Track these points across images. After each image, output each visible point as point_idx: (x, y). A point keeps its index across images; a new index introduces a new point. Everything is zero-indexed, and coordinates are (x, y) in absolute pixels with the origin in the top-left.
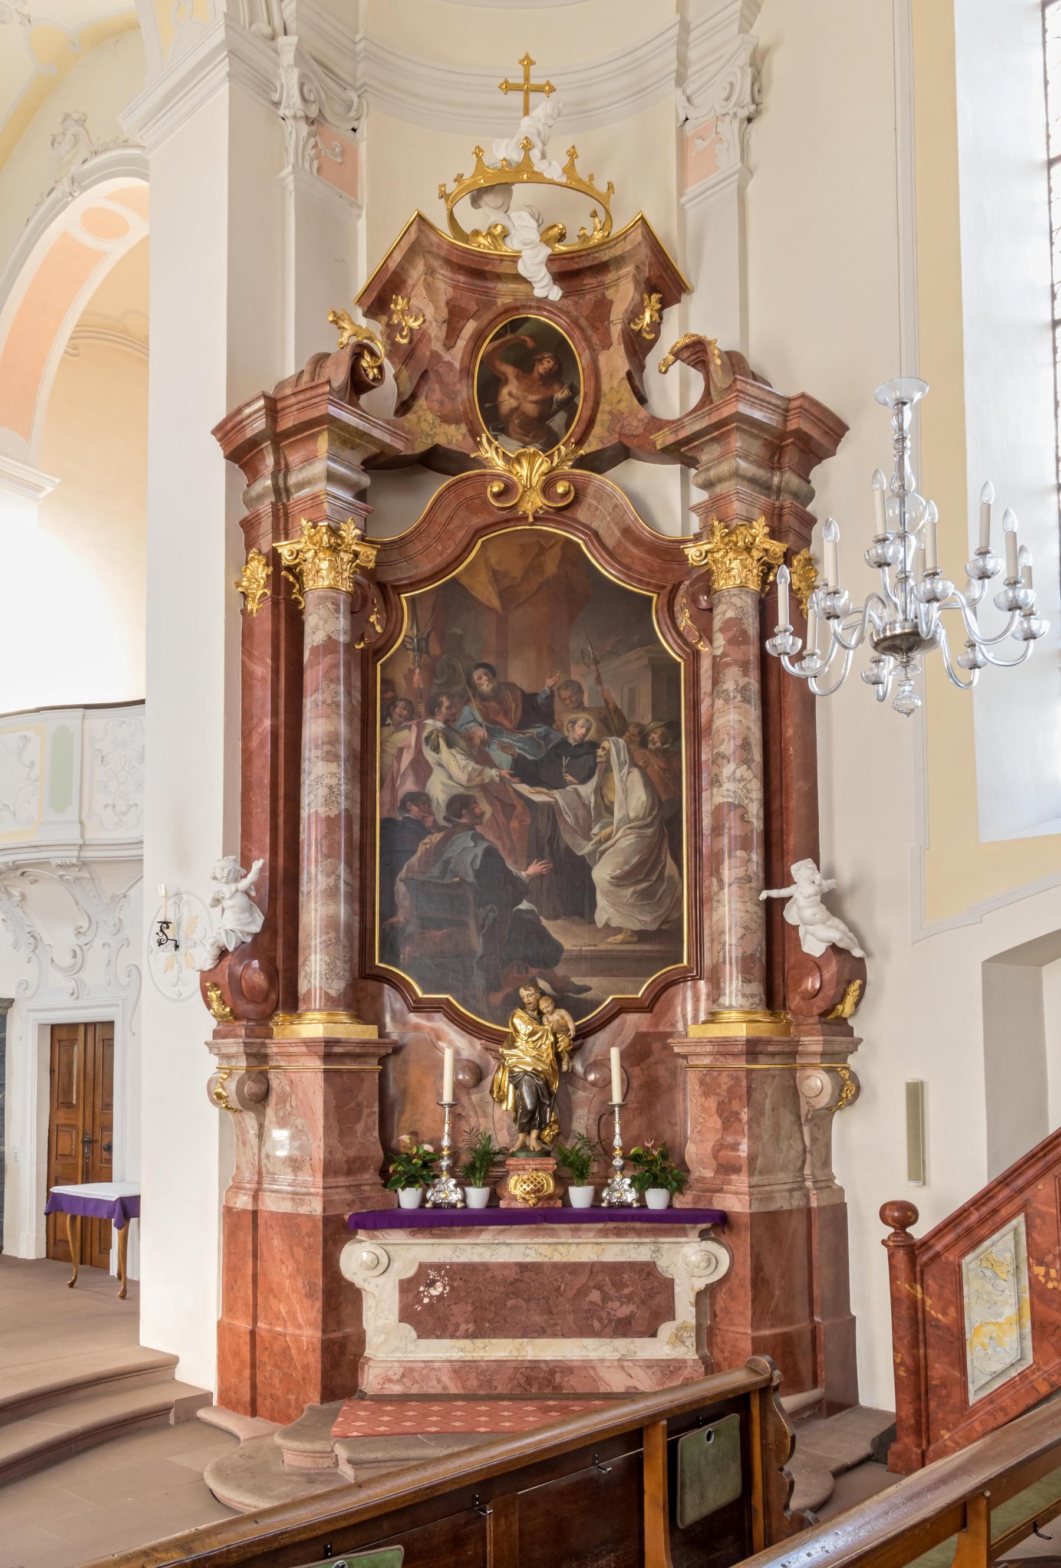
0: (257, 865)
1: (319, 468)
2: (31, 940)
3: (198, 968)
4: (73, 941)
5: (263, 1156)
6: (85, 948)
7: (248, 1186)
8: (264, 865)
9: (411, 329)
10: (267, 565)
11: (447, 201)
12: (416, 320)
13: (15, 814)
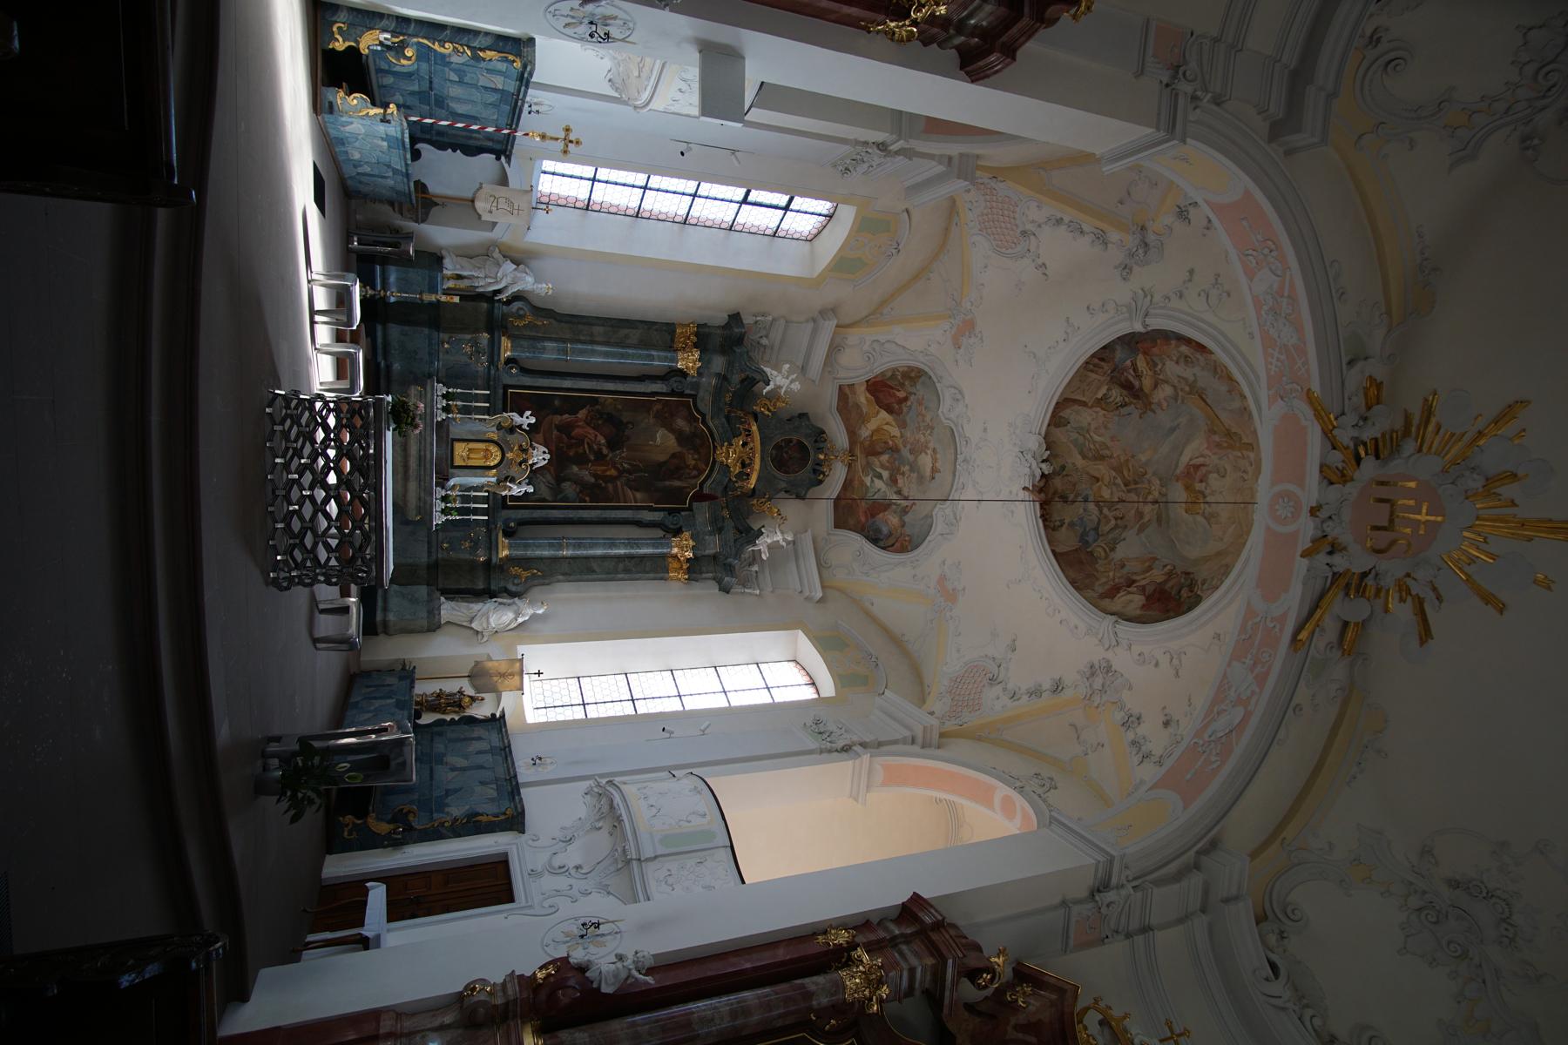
0: (649, 979)
1: (914, 961)
2: (568, 838)
3: (571, 953)
4: (571, 864)
5: (423, 1033)
6: (567, 874)
7: (399, 1025)
8: (651, 984)
9: (1017, 1000)
10: (847, 942)
11: (1094, 1003)
12: (1023, 1002)
13: (655, 816)
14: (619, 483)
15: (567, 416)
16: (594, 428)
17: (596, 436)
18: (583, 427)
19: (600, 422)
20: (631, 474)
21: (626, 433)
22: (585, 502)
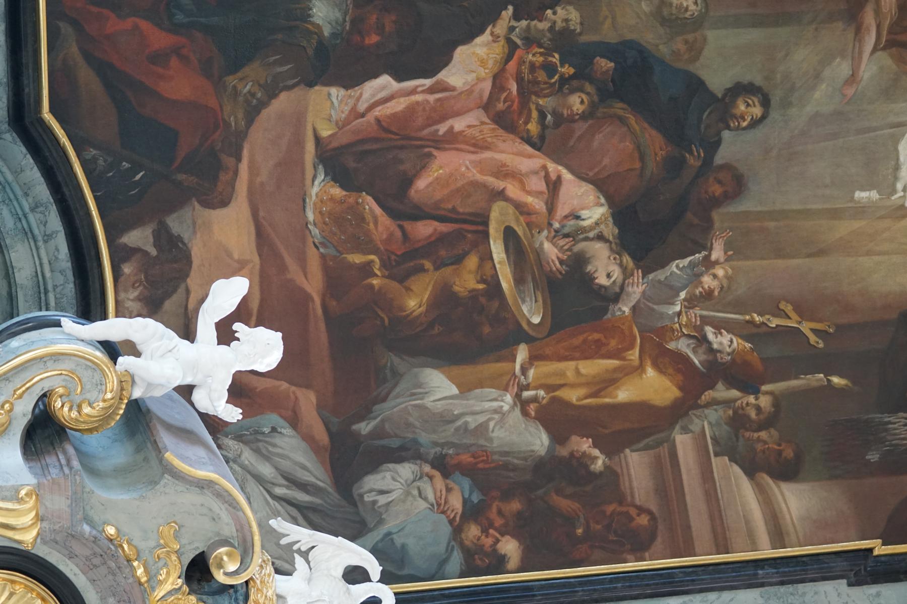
14: (683, 441)
15: (385, 83)
16: (538, 144)
17: (554, 186)
18: (479, 146)
19: (577, 103)
20: (750, 386)
21: (720, 158)
22: (498, 564)
